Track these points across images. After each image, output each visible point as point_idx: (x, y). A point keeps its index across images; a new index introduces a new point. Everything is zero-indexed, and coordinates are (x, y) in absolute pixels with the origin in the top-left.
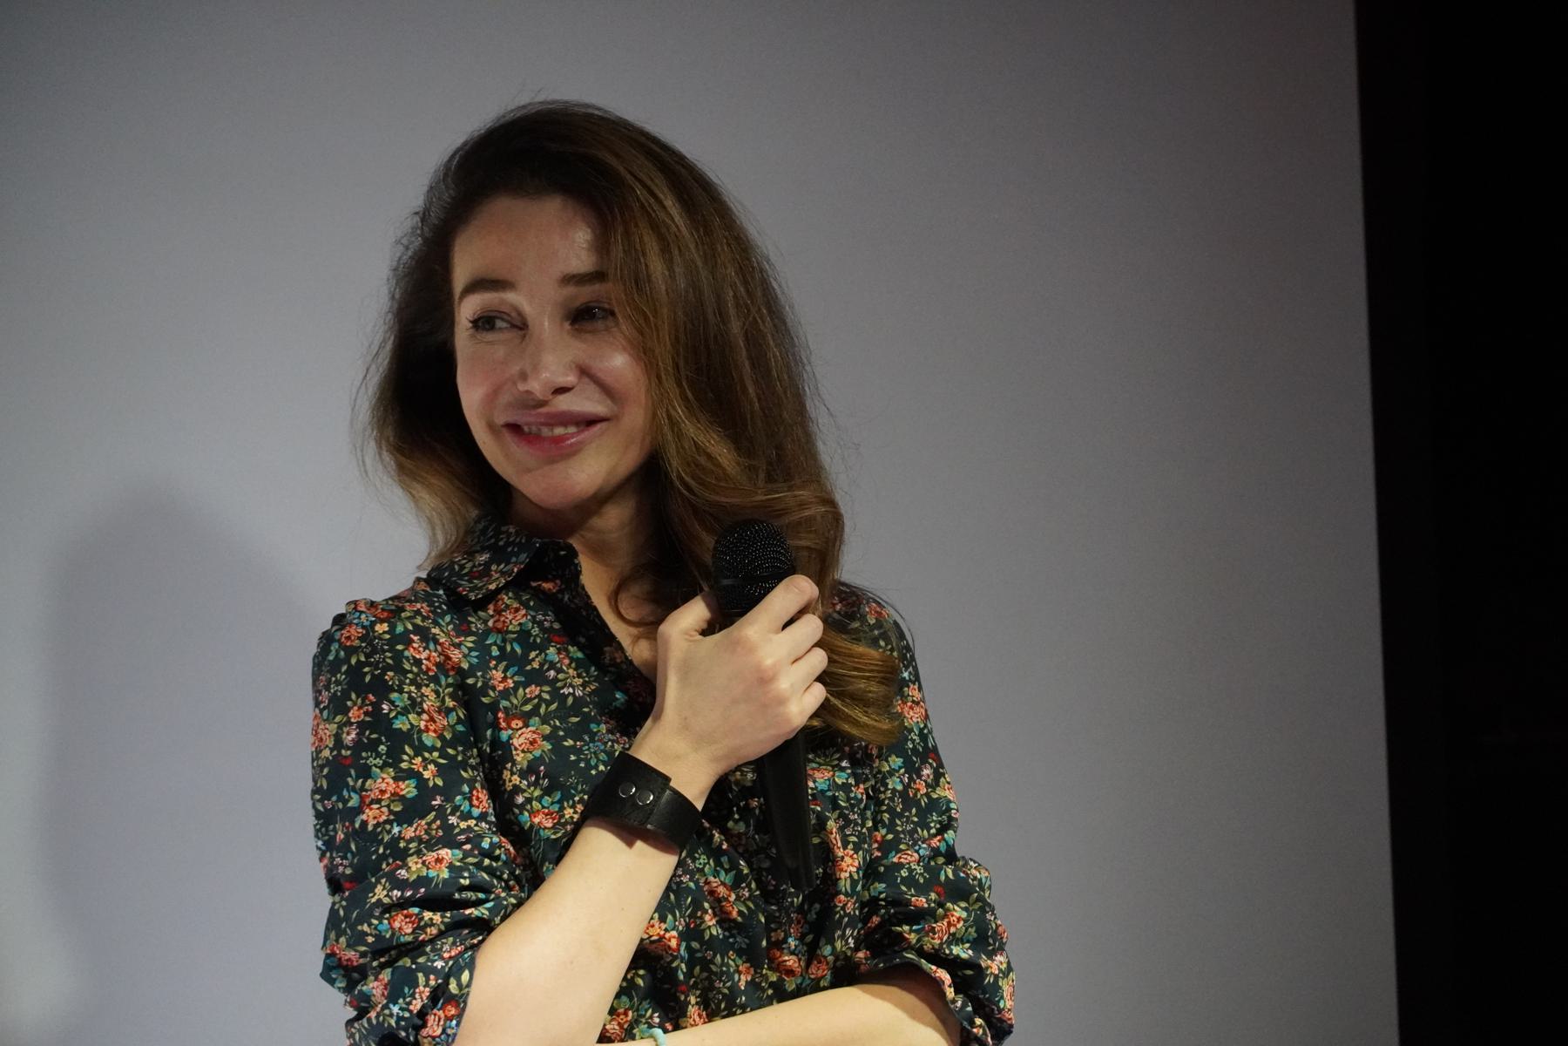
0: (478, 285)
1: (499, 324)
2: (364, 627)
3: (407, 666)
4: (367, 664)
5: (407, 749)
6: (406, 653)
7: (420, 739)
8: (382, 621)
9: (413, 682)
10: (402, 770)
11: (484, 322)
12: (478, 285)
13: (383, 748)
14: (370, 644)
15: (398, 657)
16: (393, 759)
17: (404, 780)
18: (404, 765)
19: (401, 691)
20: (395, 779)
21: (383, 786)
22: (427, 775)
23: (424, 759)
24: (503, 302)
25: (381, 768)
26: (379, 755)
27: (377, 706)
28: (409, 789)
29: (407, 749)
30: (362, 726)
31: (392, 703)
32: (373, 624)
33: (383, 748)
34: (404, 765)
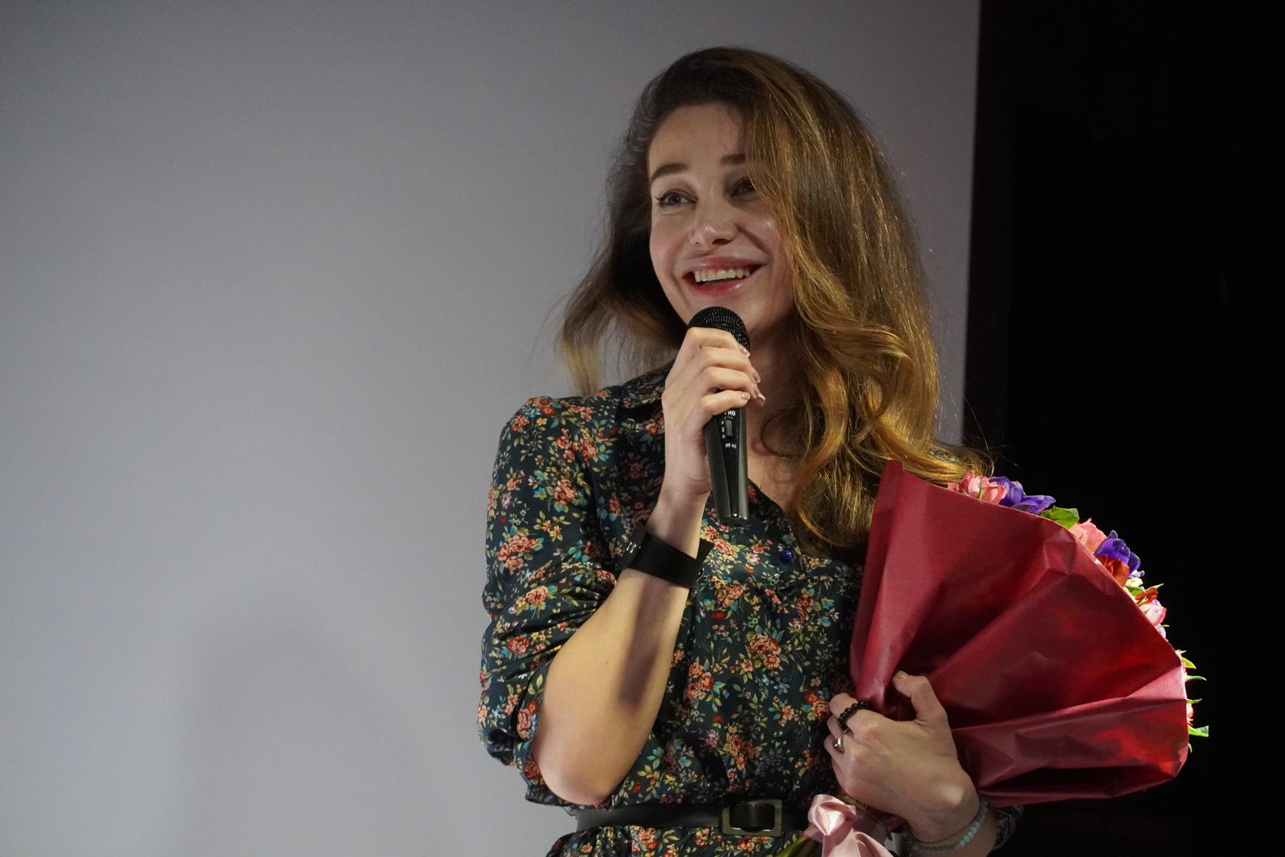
0: (666, 169)
1: (683, 200)
2: (530, 419)
3: (552, 452)
4: (525, 447)
5: (541, 514)
6: (554, 444)
7: (552, 506)
8: (544, 416)
9: (555, 464)
10: (535, 531)
11: (672, 198)
12: (666, 169)
13: (523, 512)
14: (530, 433)
15: (547, 445)
16: (529, 523)
17: (535, 538)
18: (536, 527)
19: (543, 470)
20: (530, 538)
21: (520, 542)
22: (552, 534)
23: (553, 522)
24: (682, 182)
25: (519, 527)
26: (519, 517)
27: (525, 480)
28: (538, 544)
29: (541, 514)
30: (514, 493)
31: (535, 477)
32: (537, 417)
33: (523, 512)
34: (536, 527)
